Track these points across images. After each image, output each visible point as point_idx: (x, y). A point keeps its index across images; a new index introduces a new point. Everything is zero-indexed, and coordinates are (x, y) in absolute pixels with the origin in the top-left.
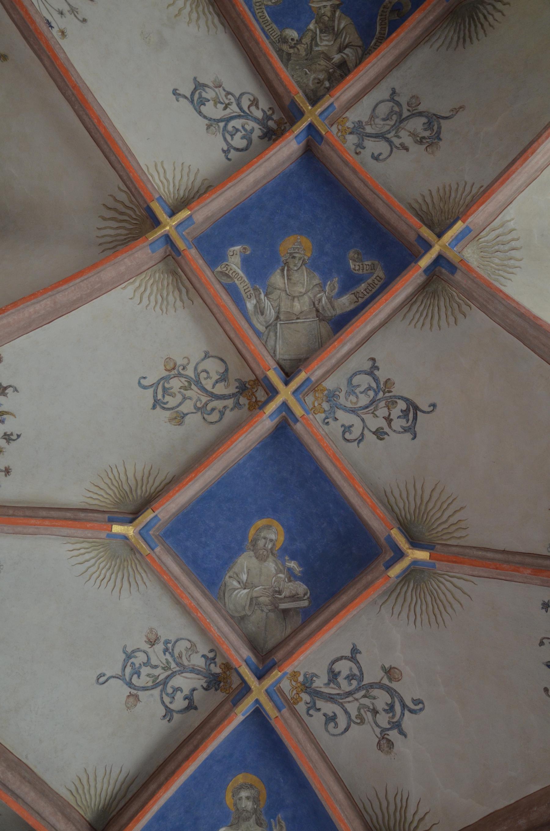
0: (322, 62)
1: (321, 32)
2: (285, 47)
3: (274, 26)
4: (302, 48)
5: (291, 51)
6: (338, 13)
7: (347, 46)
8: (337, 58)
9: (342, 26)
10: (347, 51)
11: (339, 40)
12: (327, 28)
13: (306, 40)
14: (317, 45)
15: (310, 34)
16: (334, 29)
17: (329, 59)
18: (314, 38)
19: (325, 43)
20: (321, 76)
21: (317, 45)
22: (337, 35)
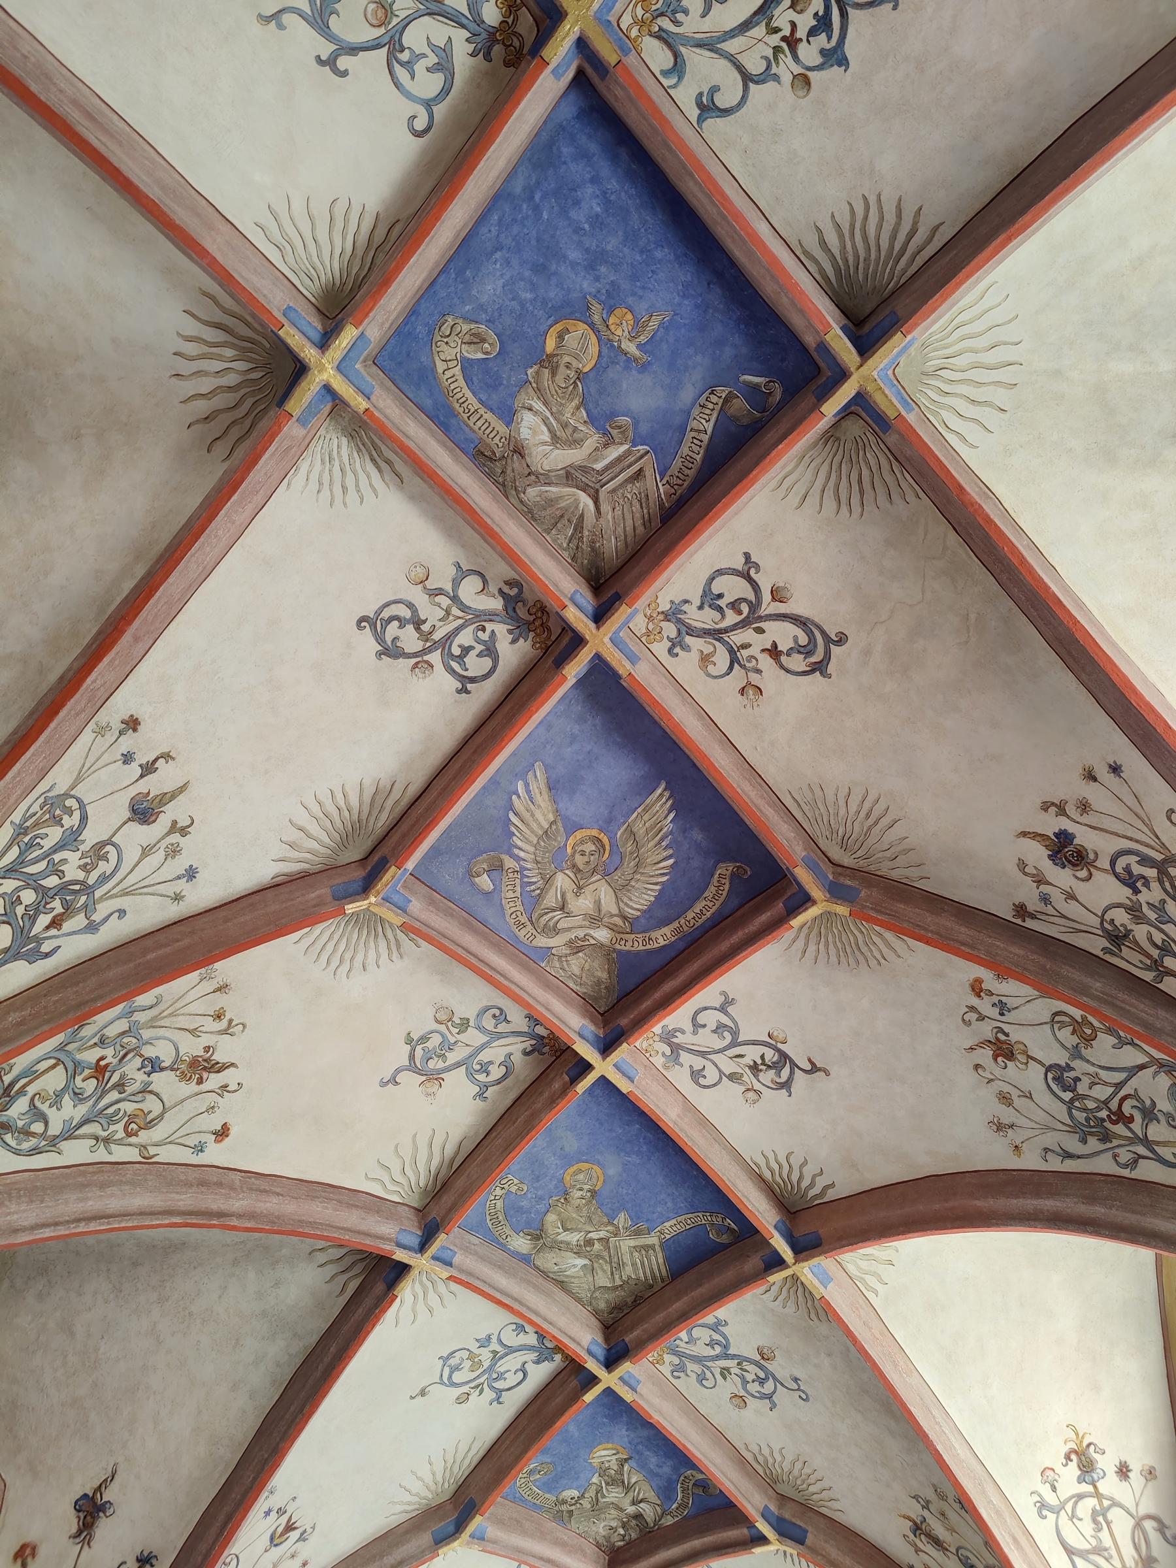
0: (612, 1511)
1: (607, 1484)
2: (564, 1508)
3: (547, 1496)
4: (586, 1504)
5: (573, 1508)
6: (626, 1467)
7: (641, 1502)
8: (631, 1510)
9: (633, 1480)
10: (641, 1505)
11: (631, 1494)
12: (616, 1481)
13: (591, 1493)
14: (604, 1496)
15: (594, 1487)
16: (623, 1482)
17: (622, 1510)
18: (599, 1491)
19: (614, 1495)
20: (614, 1524)
21: (604, 1496)
22: (628, 1489)
